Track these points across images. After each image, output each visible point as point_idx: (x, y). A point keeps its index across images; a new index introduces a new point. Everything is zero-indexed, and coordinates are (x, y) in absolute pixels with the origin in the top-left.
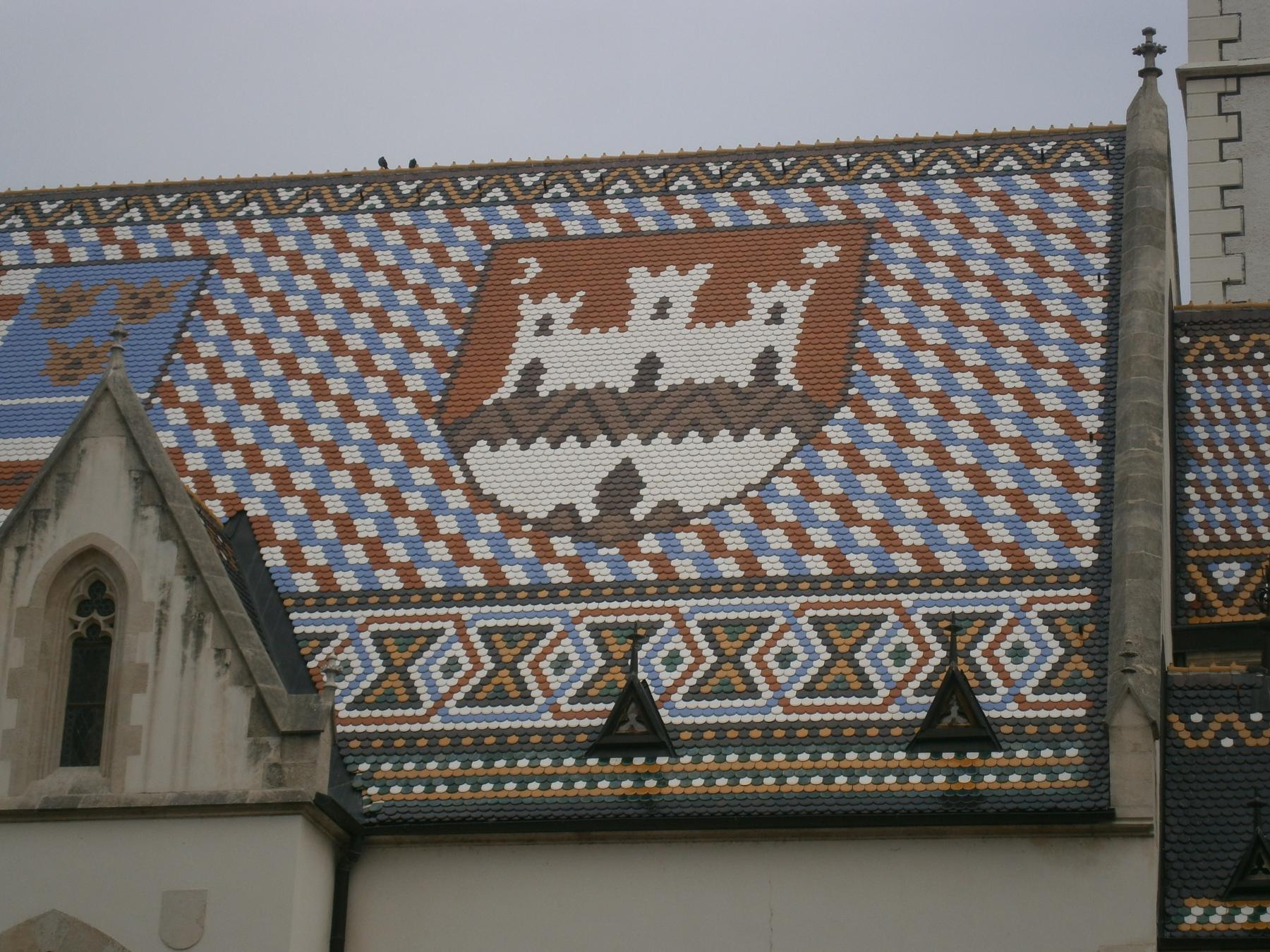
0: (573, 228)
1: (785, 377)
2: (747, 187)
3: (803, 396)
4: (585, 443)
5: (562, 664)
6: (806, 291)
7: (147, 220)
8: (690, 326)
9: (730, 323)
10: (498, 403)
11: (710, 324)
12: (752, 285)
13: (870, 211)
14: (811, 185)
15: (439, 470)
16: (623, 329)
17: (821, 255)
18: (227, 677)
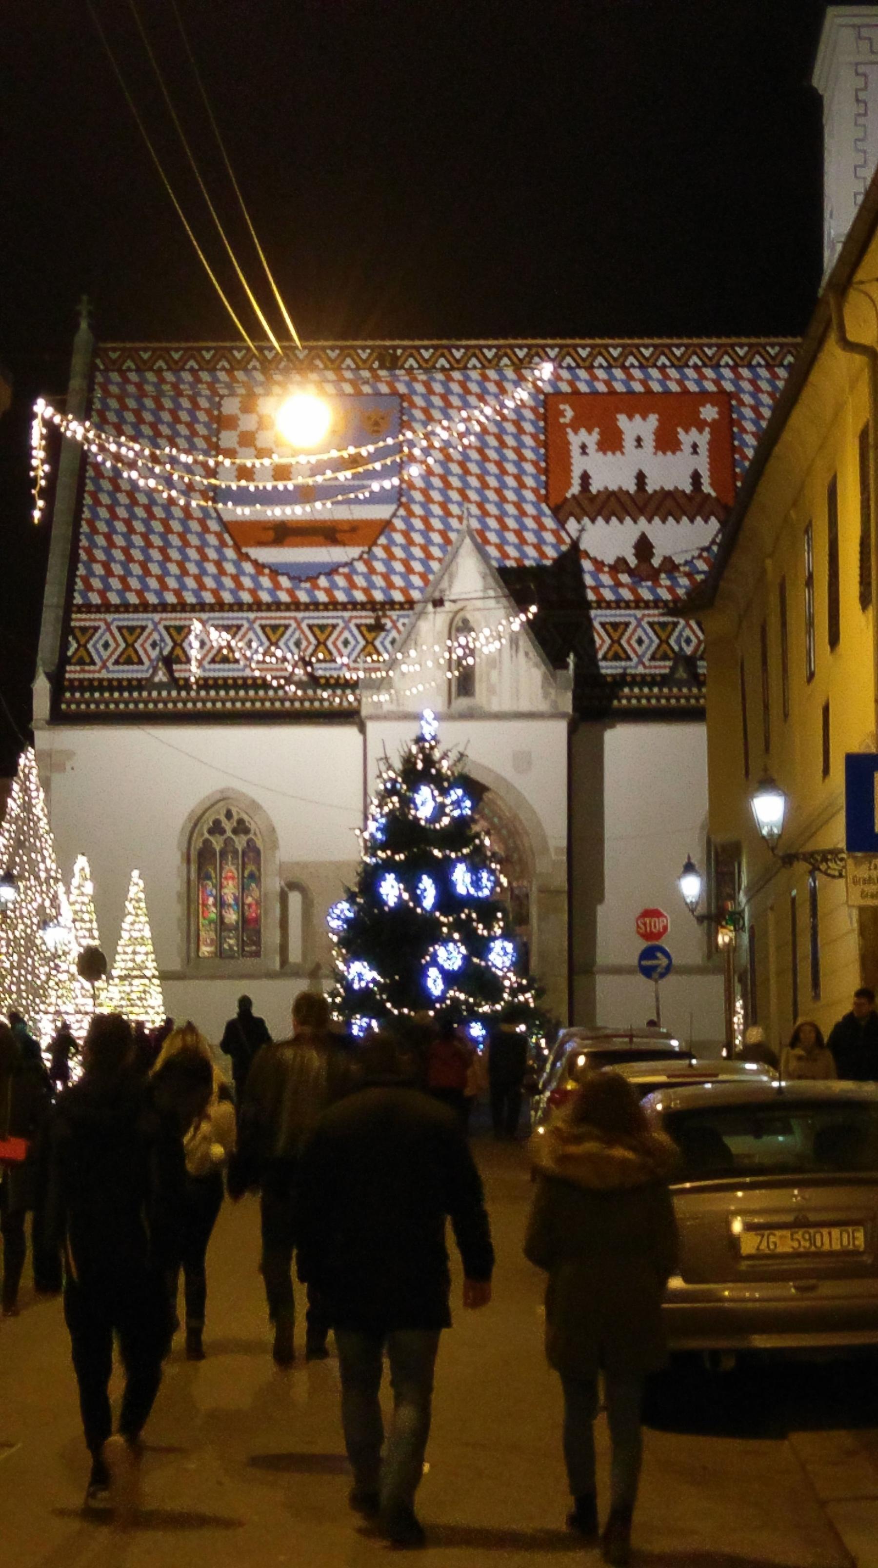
0: (583, 388)
1: (707, 488)
2: (664, 366)
3: (717, 499)
4: (621, 521)
5: (640, 641)
6: (706, 435)
7: (358, 368)
8: (655, 454)
9: (674, 453)
10: (574, 496)
11: (664, 453)
12: (679, 430)
13: (728, 387)
14: (696, 367)
15: (555, 533)
16: (623, 453)
17: (709, 413)
18: (531, 663)
